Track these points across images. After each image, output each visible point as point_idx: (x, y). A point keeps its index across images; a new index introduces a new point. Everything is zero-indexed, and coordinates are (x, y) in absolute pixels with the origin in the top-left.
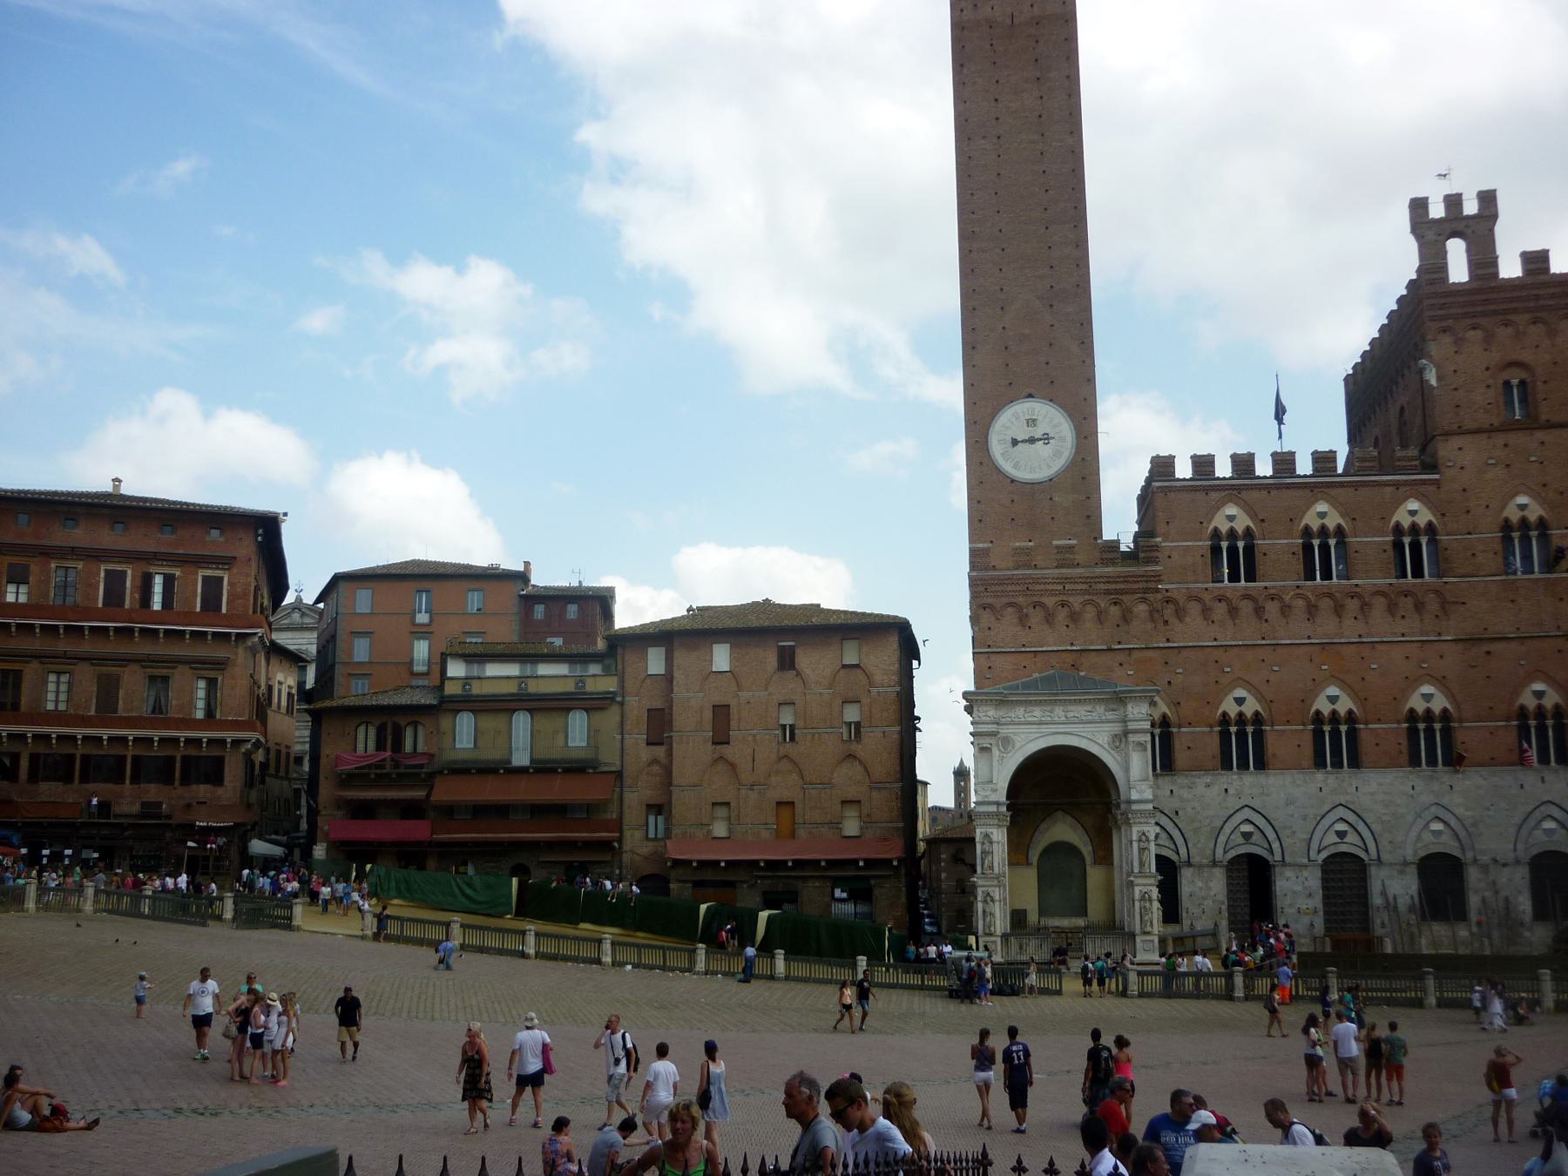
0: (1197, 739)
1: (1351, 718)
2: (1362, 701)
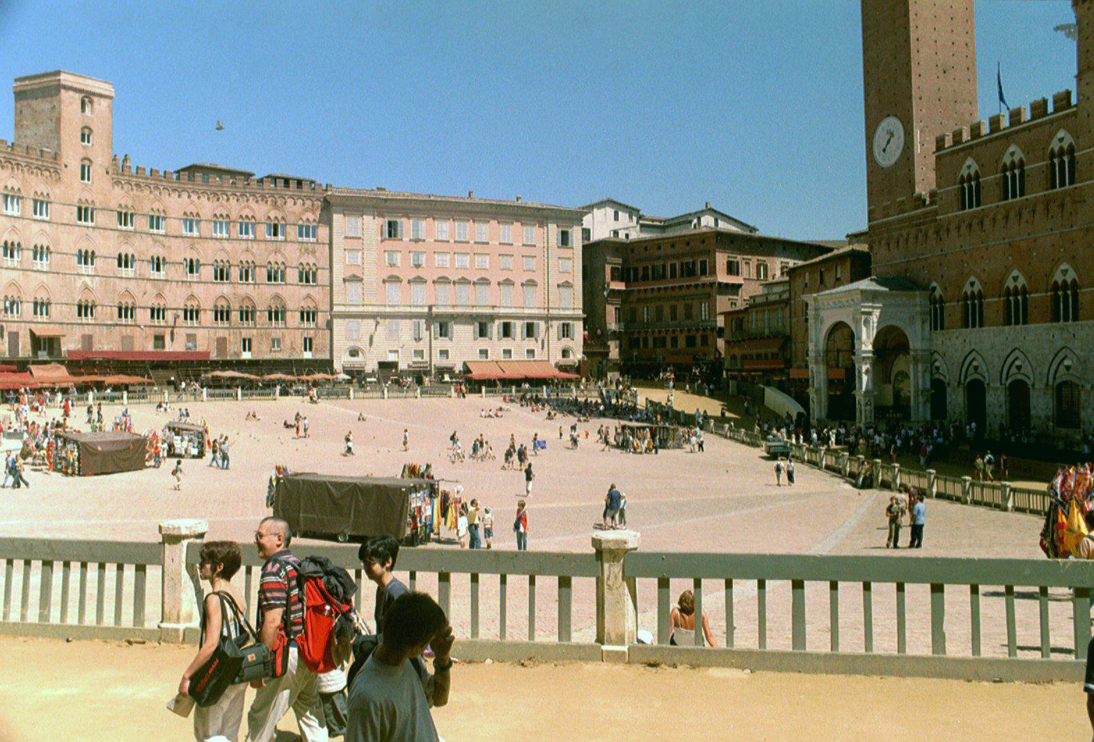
0: (953, 309)
1: (1024, 291)
2: (1029, 278)
